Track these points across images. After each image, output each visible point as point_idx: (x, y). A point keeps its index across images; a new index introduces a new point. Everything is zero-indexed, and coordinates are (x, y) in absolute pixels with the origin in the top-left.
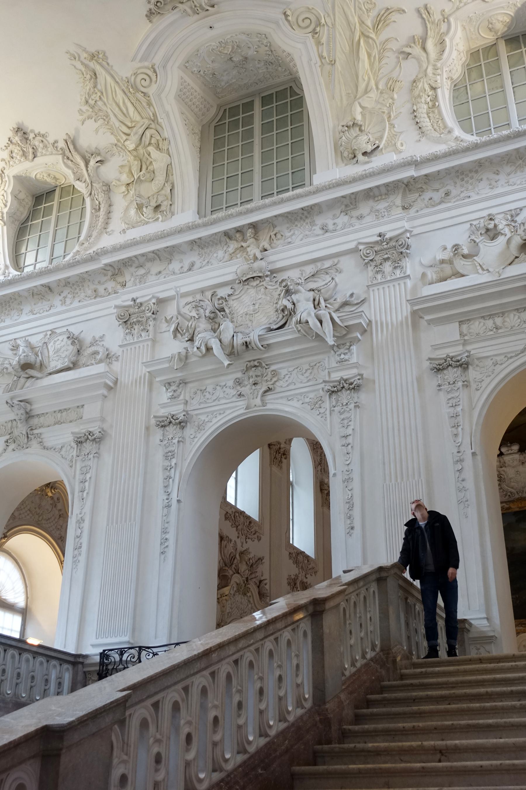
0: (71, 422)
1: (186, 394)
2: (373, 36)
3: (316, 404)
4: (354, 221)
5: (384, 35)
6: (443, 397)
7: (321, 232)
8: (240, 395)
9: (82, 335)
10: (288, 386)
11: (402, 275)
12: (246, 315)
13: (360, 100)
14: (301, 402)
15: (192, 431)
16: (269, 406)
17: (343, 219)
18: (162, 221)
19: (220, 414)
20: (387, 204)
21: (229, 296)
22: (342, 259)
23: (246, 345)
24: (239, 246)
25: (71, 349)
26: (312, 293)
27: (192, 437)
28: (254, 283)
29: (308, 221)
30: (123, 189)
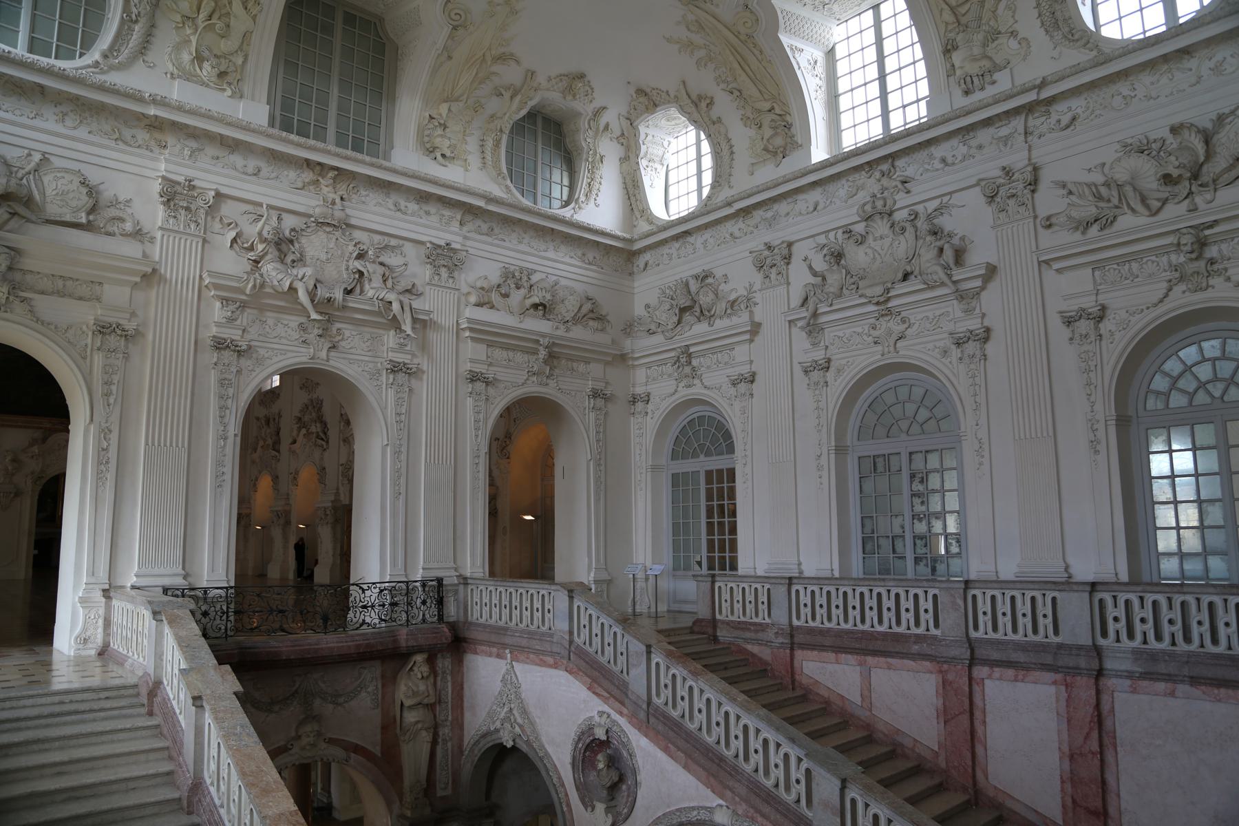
0: (80, 299)
1: (245, 318)
2: (489, 63)
4: (422, 213)
5: (496, 68)
6: (469, 401)
7: (392, 207)
8: (304, 342)
9: (102, 187)
10: (350, 348)
13: (452, 104)
14: (360, 369)
15: (249, 363)
16: (331, 363)
17: (413, 206)
18: (229, 97)
19: (281, 354)
20: (449, 214)
21: (302, 230)
22: (405, 242)
23: (329, 300)
25: (84, 200)
26: (383, 268)
27: (250, 368)
28: (328, 229)
30: (179, 19)
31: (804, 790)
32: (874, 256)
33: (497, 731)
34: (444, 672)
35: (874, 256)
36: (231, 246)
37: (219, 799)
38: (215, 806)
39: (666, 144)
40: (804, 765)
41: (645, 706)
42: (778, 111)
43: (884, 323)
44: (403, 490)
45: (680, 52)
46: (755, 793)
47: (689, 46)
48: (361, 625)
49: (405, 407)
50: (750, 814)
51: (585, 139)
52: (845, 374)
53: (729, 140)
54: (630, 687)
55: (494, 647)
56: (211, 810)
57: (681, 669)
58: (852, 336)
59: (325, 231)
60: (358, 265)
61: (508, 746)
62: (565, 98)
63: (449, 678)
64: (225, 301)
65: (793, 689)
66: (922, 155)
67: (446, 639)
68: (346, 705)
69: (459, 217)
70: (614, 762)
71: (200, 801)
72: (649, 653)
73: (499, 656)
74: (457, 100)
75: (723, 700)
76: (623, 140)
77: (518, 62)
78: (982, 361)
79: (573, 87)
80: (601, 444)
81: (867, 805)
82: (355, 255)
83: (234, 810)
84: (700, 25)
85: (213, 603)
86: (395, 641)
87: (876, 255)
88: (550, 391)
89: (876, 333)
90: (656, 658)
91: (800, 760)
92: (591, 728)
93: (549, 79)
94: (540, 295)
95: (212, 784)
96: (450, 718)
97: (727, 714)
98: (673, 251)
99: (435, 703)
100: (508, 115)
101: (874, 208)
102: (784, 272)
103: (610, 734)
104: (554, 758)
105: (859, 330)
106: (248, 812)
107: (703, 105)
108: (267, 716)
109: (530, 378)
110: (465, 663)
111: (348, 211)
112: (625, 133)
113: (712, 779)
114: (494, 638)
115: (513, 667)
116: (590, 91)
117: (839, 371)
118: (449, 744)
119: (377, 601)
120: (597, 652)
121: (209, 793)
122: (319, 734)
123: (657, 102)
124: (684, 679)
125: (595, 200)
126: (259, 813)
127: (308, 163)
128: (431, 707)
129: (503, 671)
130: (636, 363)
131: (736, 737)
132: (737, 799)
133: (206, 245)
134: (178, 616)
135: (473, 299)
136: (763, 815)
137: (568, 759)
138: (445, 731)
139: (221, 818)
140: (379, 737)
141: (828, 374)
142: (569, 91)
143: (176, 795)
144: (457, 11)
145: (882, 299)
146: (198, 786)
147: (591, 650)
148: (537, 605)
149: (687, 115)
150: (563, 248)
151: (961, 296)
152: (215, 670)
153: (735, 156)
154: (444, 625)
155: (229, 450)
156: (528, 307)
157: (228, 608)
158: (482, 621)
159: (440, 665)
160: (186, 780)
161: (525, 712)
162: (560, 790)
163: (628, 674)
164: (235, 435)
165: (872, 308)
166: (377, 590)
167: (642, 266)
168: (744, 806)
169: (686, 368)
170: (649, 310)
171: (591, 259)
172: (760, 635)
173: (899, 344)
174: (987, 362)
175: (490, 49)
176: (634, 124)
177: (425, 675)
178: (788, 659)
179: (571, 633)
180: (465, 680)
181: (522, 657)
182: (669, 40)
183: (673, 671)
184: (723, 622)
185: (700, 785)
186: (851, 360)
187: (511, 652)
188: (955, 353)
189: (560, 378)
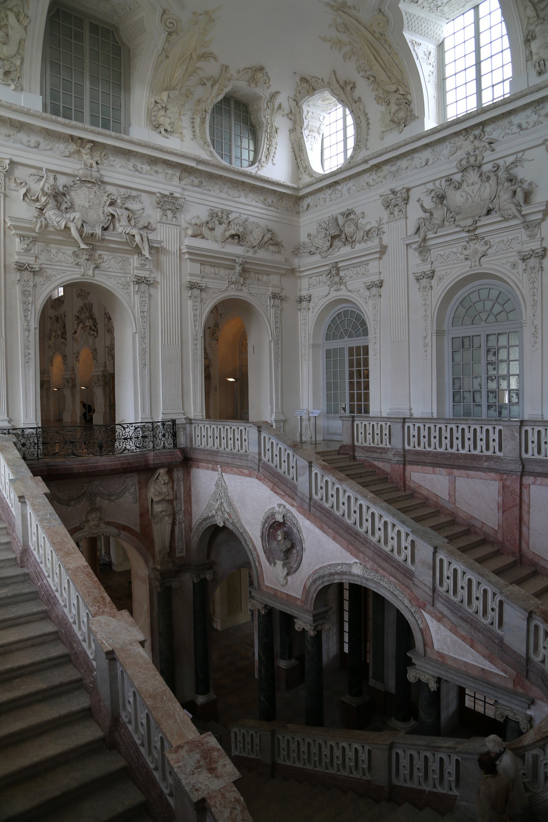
1: (37, 249)
3: (126, 286)
4: (153, 172)
5: (199, 64)
6: (190, 303)
7: (132, 169)
8: (77, 264)
10: (108, 268)
11: (176, 223)
12: (83, 207)
13: (170, 92)
15: (41, 279)
16: (96, 278)
17: (146, 168)
18: (13, 90)
19: (62, 273)
21: (71, 186)
22: (143, 194)
23: (92, 235)
24: (77, 149)
26: (128, 212)
27: (42, 283)
28: (89, 185)
29: (127, 157)
31: (410, 553)
32: (467, 197)
33: (213, 516)
34: (178, 480)
35: (467, 197)
36: (24, 199)
37: (40, 558)
38: (37, 562)
39: (321, 118)
40: (410, 538)
41: (308, 501)
42: (401, 92)
43: (472, 245)
44: (147, 363)
45: (331, 48)
46: (378, 555)
47: (338, 43)
48: (124, 451)
49: (146, 307)
50: (374, 568)
51: (264, 116)
52: (444, 281)
53: (366, 115)
54: (299, 488)
55: (210, 463)
56: (35, 565)
57: (331, 477)
58: (450, 254)
59: (87, 187)
60: (111, 210)
61: (221, 526)
62: (250, 85)
63: (182, 483)
64: (22, 237)
65: (405, 490)
66: (504, 122)
67: (179, 458)
68: (116, 501)
69: (178, 174)
70: (288, 535)
71: (28, 559)
72: (310, 467)
73: (213, 469)
74: (174, 89)
75: (359, 497)
76: (291, 116)
77: (216, 59)
78: (540, 272)
79: (255, 77)
80: (278, 330)
81: (450, 563)
82: (108, 203)
83: (49, 565)
84: (346, 26)
85: (28, 437)
86: (146, 460)
87: (469, 197)
88: (243, 295)
89: (466, 252)
90: (315, 470)
91: (407, 535)
92: (273, 515)
93: (239, 72)
94: (236, 228)
95: (35, 549)
96: (183, 509)
97: (361, 506)
98: (327, 196)
99: (173, 499)
100: (210, 99)
101: (468, 162)
102: (404, 210)
103: (285, 518)
104: (250, 533)
105: (455, 250)
106: (58, 566)
107: (348, 88)
108: (67, 508)
109: (230, 286)
110: (191, 474)
111: (102, 172)
112: (293, 111)
113: (351, 547)
114: (210, 458)
115: (222, 476)
116: (267, 80)
117: (440, 279)
118: (183, 525)
119: (133, 435)
120: (276, 467)
121: (33, 555)
122: (100, 519)
123: (315, 88)
124: (333, 484)
125: (272, 160)
126: (65, 567)
127: (72, 138)
128: (170, 502)
129: (217, 479)
130: (302, 275)
131: (367, 520)
132: (367, 559)
133: (6, 198)
134: (6, 446)
135: (190, 232)
136: (383, 569)
137: (258, 534)
138: (180, 517)
139: (41, 569)
140: (138, 521)
141: (432, 281)
142: (253, 80)
143: (13, 556)
144: (172, 21)
145: (471, 228)
146: (26, 551)
147: (273, 465)
148: (237, 436)
149: (336, 97)
150: (251, 195)
151: (527, 225)
152: (32, 479)
153: (370, 126)
154: (177, 450)
155: (32, 338)
156: (227, 236)
157: (38, 441)
158: (202, 447)
159: (176, 475)
160: (18, 547)
161: (230, 504)
162: (254, 553)
163: (297, 480)
164: (35, 328)
165: (465, 234)
166: (133, 428)
167: (305, 207)
168: (371, 563)
169: (335, 277)
170: (311, 238)
171: (270, 202)
172: (384, 456)
173: (483, 260)
174: (543, 272)
175: (195, 49)
176: (299, 104)
177: (166, 482)
178: (402, 471)
179: (260, 454)
180: (192, 485)
181: (228, 470)
182: (324, 39)
183: (326, 478)
184: (359, 447)
185: (344, 551)
186: (448, 271)
187: (221, 467)
188: (521, 266)
189: (250, 286)
